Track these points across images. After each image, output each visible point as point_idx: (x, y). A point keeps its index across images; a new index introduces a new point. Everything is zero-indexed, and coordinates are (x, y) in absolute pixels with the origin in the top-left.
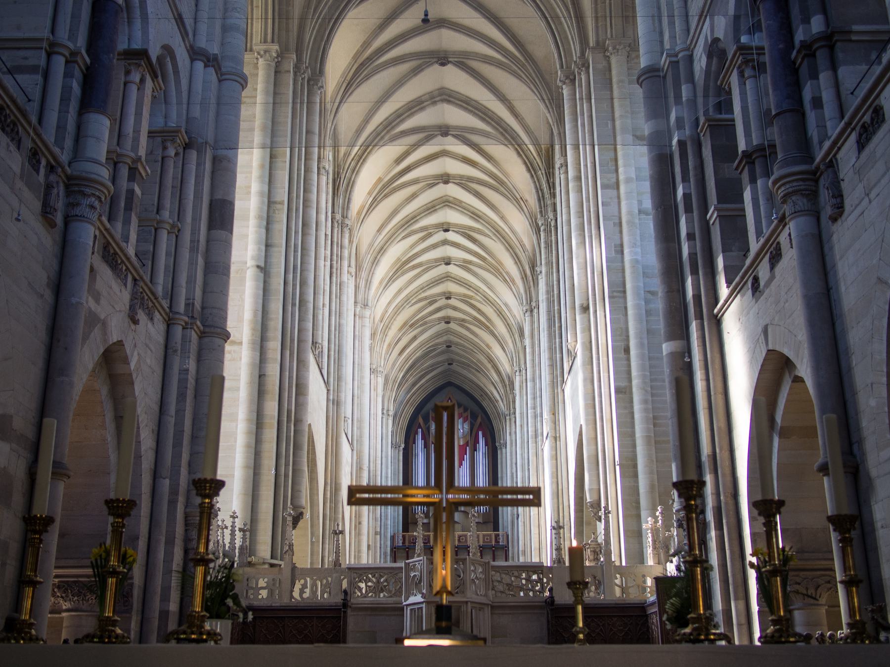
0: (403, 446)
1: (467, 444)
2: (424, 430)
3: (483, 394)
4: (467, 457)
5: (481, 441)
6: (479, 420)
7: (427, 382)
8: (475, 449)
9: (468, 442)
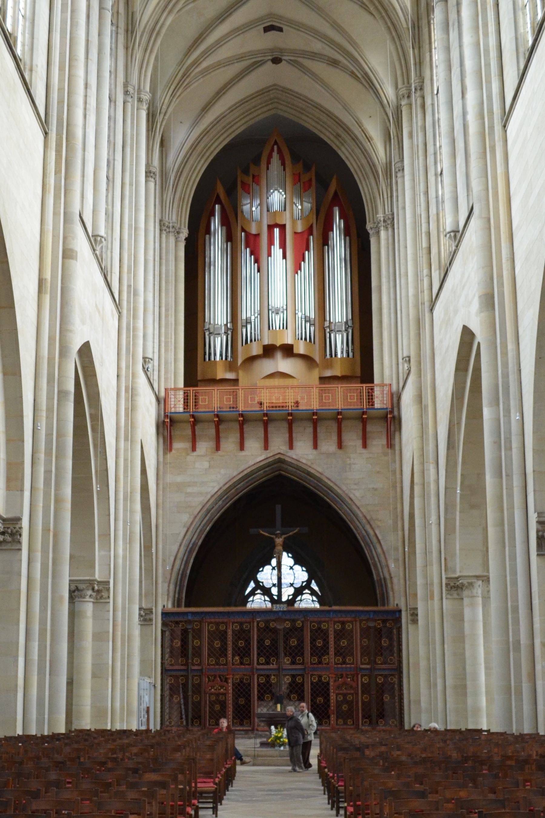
0: (185, 233)
1: (310, 230)
2: (226, 206)
3: (340, 131)
4: (310, 256)
5: (338, 223)
6: (333, 187)
7: (232, 109)
8: (325, 241)
9: (311, 227)
